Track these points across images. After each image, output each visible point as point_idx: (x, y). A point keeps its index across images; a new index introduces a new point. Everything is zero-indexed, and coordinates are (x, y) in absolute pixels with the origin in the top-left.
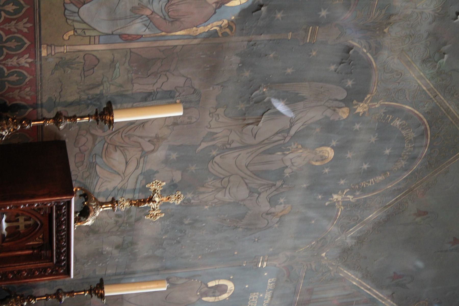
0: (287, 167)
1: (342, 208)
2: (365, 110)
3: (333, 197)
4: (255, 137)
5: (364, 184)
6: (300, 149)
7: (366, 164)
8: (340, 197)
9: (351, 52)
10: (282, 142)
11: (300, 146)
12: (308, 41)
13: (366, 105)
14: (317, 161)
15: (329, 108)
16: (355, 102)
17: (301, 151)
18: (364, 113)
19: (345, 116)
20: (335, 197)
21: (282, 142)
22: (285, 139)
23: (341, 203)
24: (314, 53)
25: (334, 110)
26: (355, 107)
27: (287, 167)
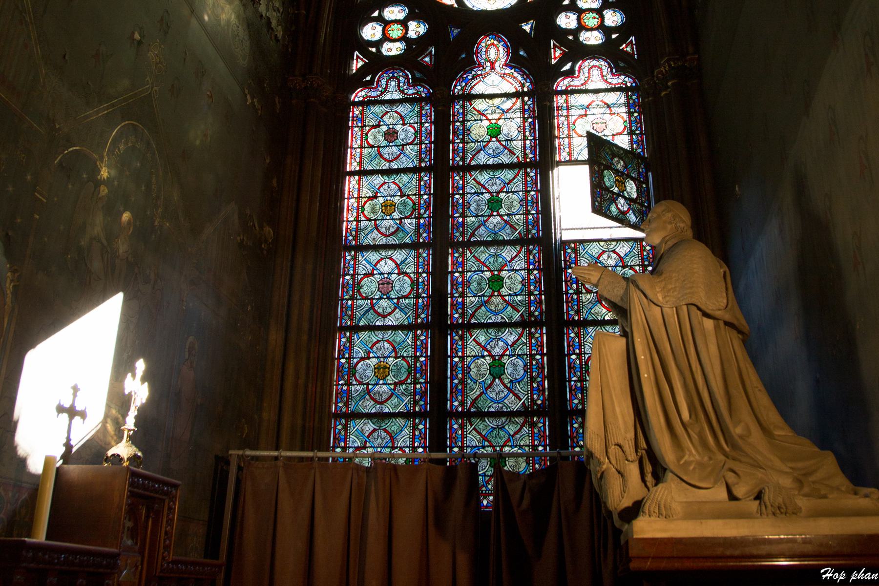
0: (127, 258)
1: (165, 220)
2: (106, 171)
3: (156, 226)
4: (100, 279)
5: (154, 195)
6: (118, 240)
7: (141, 187)
8: (157, 219)
9: (64, 165)
10: (109, 255)
11: (116, 240)
12: (45, 201)
13: (104, 169)
14: (130, 229)
15: (97, 202)
16: (99, 177)
17: (120, 240)
18: (108, 172)
19: (106, 191)
20: (156, 223)
21: (109, 255)
22: (108, 252)
23: (161, 220)
24: (56, 199)
25: (100, 198)
26: (102, 178)
27: (127, 258)
